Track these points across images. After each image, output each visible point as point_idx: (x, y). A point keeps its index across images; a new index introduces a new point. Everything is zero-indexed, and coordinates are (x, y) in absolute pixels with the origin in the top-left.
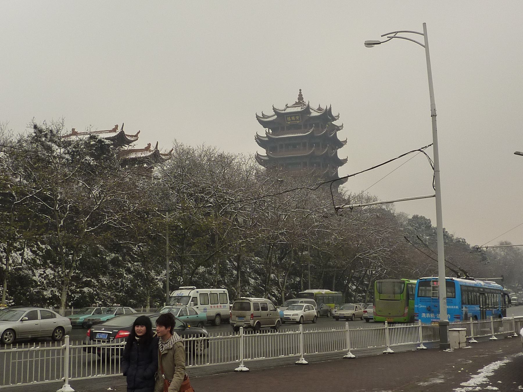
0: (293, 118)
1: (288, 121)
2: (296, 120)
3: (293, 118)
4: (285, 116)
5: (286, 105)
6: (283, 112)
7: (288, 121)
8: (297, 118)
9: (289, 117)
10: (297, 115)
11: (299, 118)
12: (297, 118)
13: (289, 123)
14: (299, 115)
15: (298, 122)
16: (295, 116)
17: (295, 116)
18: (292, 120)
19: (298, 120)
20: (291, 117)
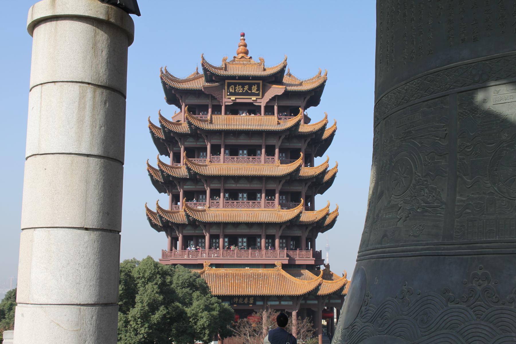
4: (227, 81)
5: (225, 60)
6: (222, 73)
10: (254, 84)
11: (258, 90)
13: (233, 98)
15: (254, 98)
17: (250, 86)
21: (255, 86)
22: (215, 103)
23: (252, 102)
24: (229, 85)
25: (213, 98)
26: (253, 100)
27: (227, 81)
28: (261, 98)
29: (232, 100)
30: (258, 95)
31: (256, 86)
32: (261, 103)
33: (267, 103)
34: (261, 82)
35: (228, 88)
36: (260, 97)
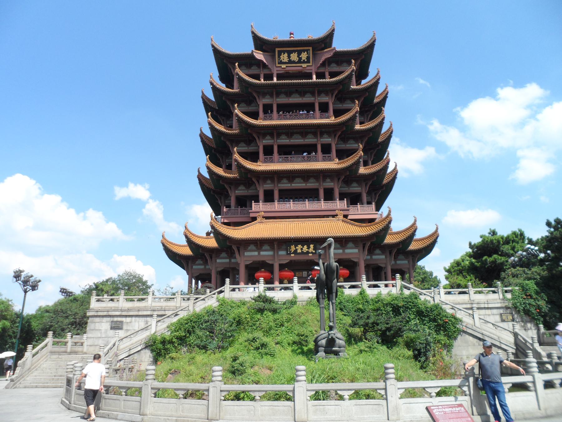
0: (294, 57)
1: (281, 63)
2: (300, 61)
3: (294, 57)
4: (277, 50)
7: (281, 63)
8: (304, 56)
9: (286, 54)
10: (304, 51)
11: (308, 58)
12: (304, 56)
13: (284, 66)
14: (307, 51)
15: (304, 65)
16: (299, 53)
17: (299, 53)
18: (290, 62)
19: (304, 62)
20: (289, 53)
21: (304, 53)
22: (266, 71)
23: (303, 69)
24: (280, 53)
25: (265, 66)
26: (303, 68)
27: (277, 50)
28: (311, 65)
29: (283, 68)
30: (308, 61)
31: (306, 53)
32: (312, 70)
33: (318, 68)
34: (311, 48)
35: (279, 57)
36: (310, 64)
